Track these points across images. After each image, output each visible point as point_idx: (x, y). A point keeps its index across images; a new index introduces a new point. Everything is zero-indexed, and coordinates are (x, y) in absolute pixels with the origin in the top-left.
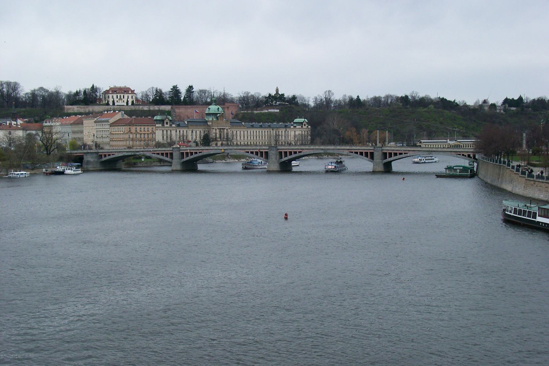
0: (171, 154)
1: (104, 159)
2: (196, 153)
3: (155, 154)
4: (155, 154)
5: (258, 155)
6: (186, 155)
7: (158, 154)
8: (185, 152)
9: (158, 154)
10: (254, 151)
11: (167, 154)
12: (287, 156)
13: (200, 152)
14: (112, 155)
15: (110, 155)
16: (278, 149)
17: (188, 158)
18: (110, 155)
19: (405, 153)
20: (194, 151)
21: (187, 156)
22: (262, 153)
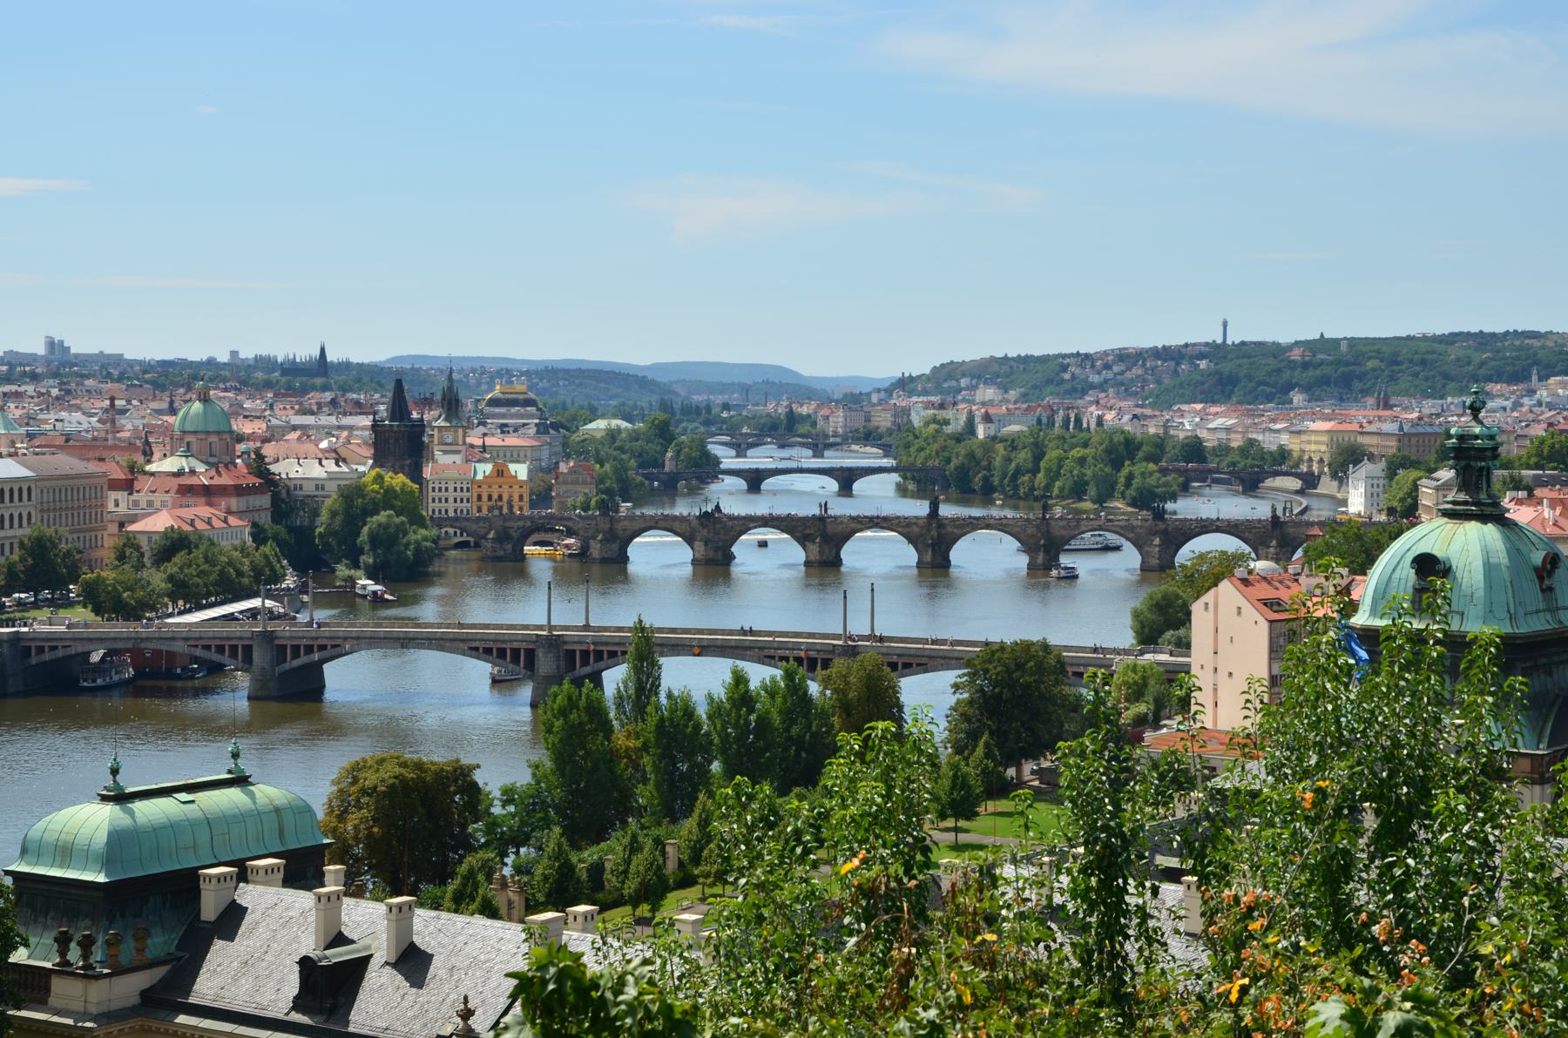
0: (248, 650)
1: (34, 661)
2: (323, 648)
3: (196, 646)
4: (196, 646)
5: (505, 659)
6: (292, 652)
7: (208, 648)
8: (289, 643)
9: (208, 648)
10: (495, 646)
11: (234, 649)
12: (588, 664)
13: (334, 646)
14: (64, 647)
15: (56, 648)
16: (565, 643)
17: (296, 663)
18: (54, 648)
19: (918, 665)
20: (316, 643)
21: (296, 654)
22: (516, 652)
